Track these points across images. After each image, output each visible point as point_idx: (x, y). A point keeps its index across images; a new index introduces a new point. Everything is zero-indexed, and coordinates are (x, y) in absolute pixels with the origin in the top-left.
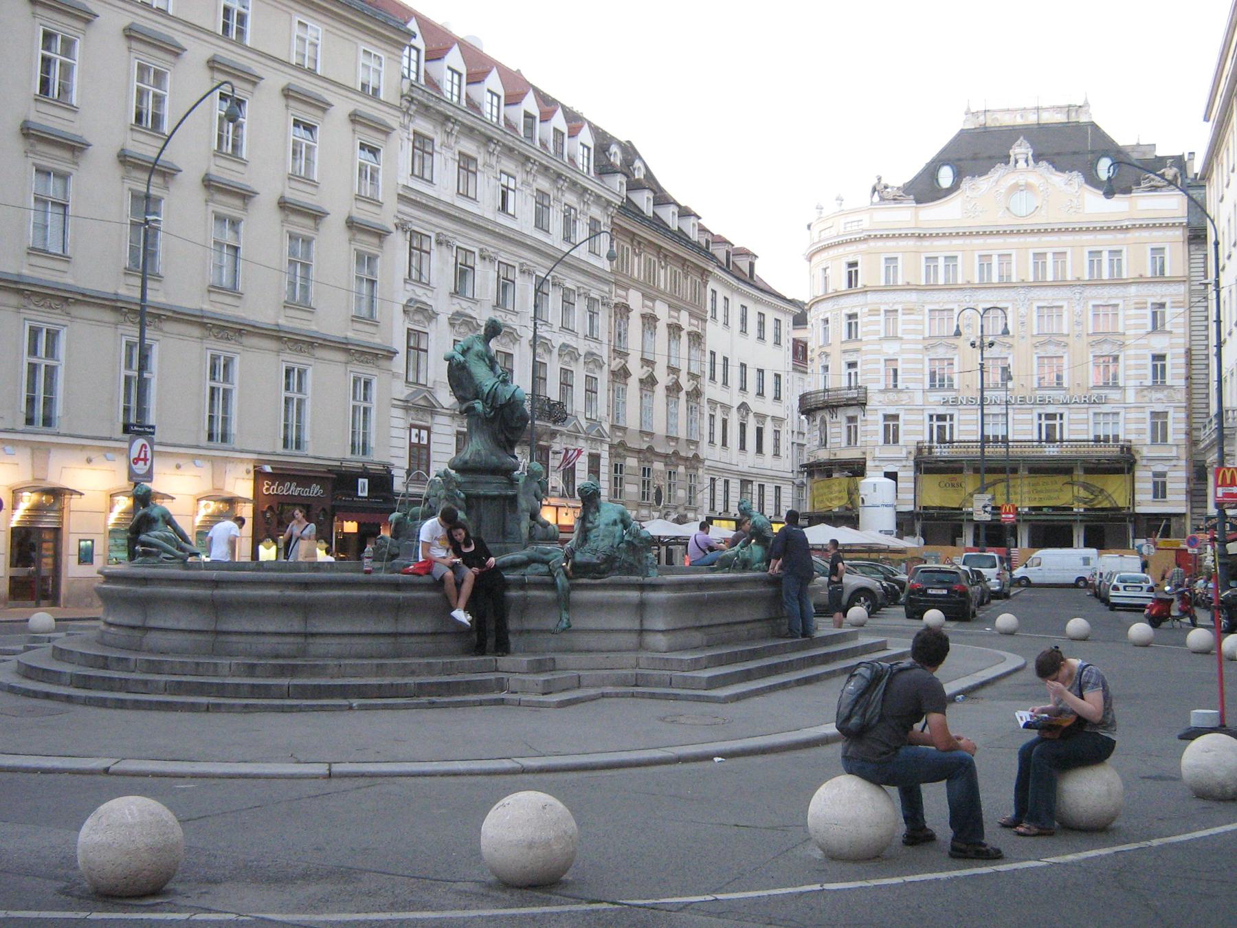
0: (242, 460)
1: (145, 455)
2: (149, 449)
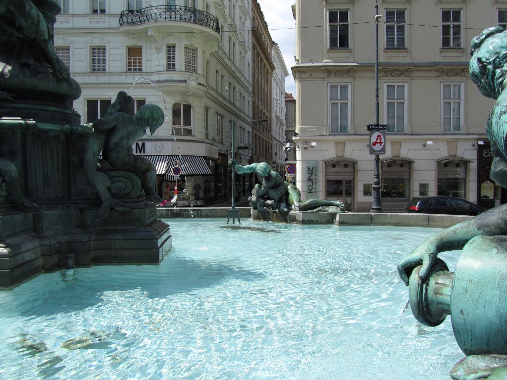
0: (469, 140)
1: (381, 140)
2: (382, 137)
